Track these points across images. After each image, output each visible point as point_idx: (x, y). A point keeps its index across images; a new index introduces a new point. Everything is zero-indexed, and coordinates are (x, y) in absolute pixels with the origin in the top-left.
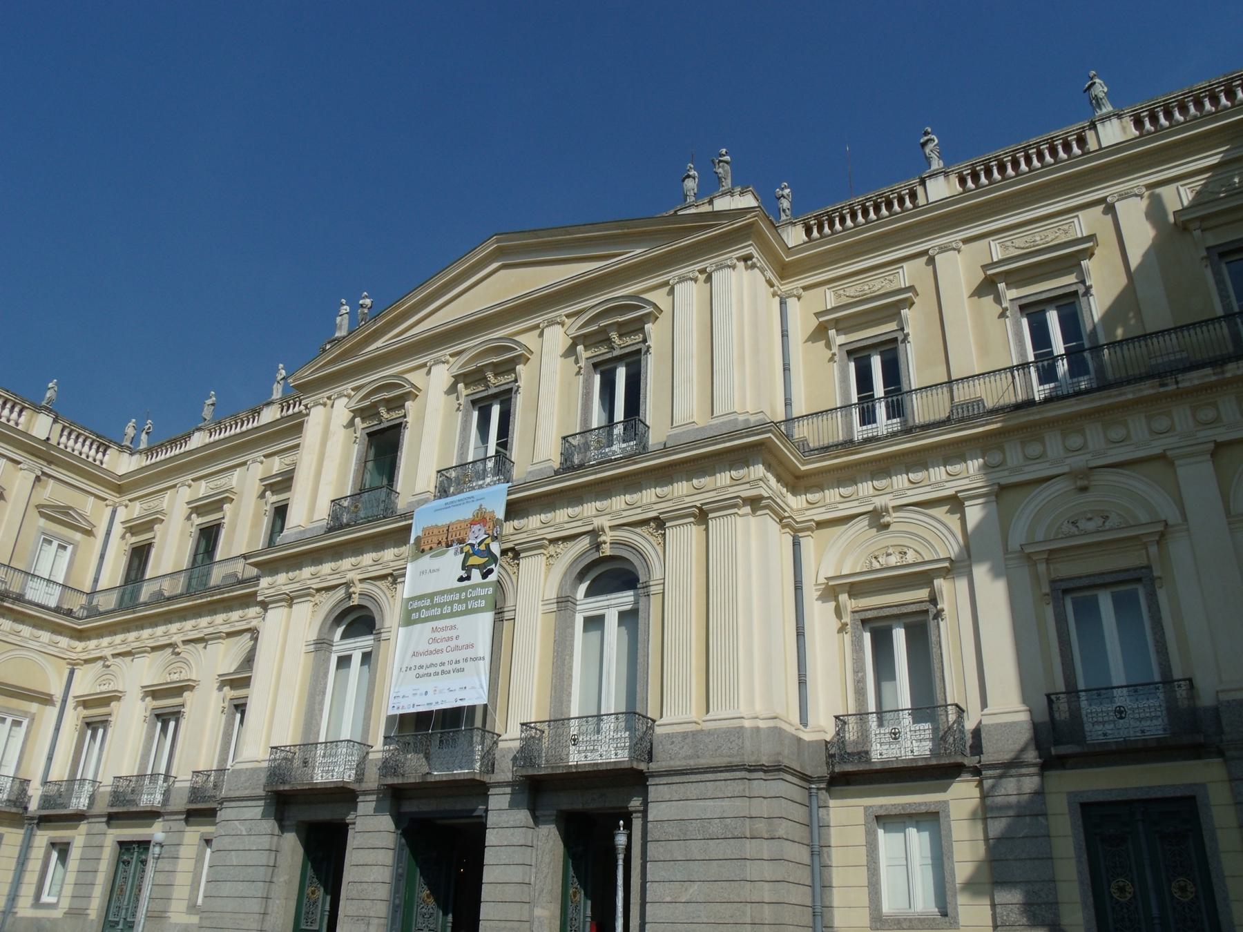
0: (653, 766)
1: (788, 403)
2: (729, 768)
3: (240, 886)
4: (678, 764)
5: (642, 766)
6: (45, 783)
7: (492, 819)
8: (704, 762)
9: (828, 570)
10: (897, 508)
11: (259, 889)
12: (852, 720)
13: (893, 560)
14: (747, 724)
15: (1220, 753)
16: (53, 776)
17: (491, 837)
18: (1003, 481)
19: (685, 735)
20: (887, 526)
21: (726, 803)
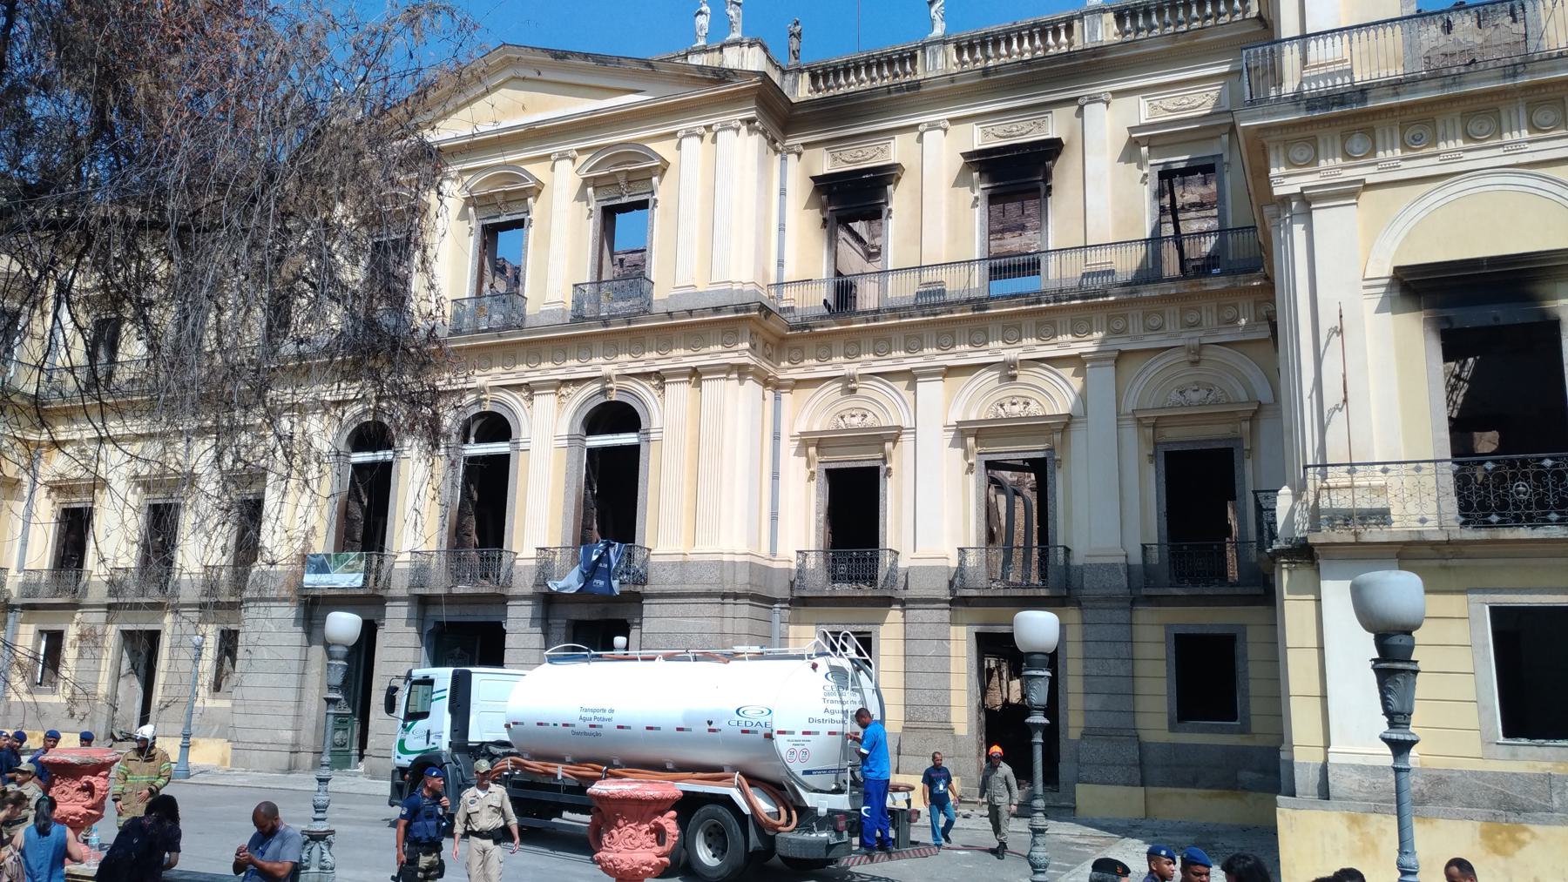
0: (648, 589)
1: (781, 263)
2: (708, 595)
3: (274, 678)
4: (669, 588)
5: (639, 589)
6: (21, 569)
7: (509, 626)
8: (689, 587)
9: (802, 427)
10: (864, 377)
11: (293, 680)
12: (812, 555)
13: (856, 421)
14: (726, 558)
15: (1079, 604)
16: (31, 564)
17: (510, 641)
18: (950, 363)
19: (674, 564)
20: (854, 391)
21: (704, 621)
